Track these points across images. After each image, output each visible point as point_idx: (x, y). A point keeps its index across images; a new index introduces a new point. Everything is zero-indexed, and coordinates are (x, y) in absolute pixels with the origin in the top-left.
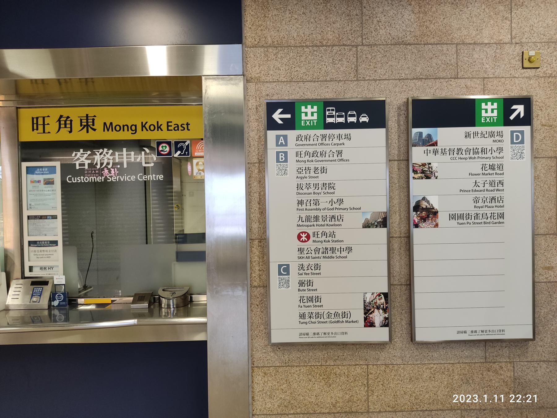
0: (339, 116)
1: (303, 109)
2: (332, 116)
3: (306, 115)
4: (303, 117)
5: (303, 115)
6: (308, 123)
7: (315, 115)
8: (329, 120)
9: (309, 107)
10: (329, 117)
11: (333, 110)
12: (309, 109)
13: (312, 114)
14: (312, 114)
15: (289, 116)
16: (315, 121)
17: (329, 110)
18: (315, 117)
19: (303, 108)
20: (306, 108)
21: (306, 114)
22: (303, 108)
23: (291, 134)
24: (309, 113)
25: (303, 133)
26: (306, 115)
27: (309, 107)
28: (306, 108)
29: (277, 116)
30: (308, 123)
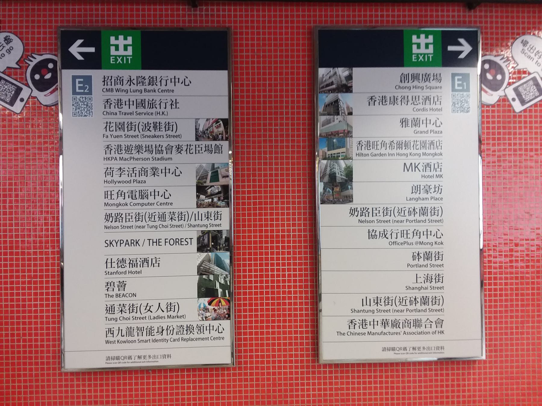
1: (113, 40)
3: (117, 48)
5: (113, 49)
6: (119, 60)
9: (121, 37)
12: (121, 41)
13: (125, 48)
14: (125, 48)
15: (92, 50)
16: (130, 58)
18: (130, 51)
19: (112, 39)
20: (117, 39)
21: (117, 48)
22: (112, 39)
23: (97, 75)
24: (122, 46)
25: (115, 73)
27: (121, 37)
28: (117, 39)
29: (75, 50)
30: (119, 60)
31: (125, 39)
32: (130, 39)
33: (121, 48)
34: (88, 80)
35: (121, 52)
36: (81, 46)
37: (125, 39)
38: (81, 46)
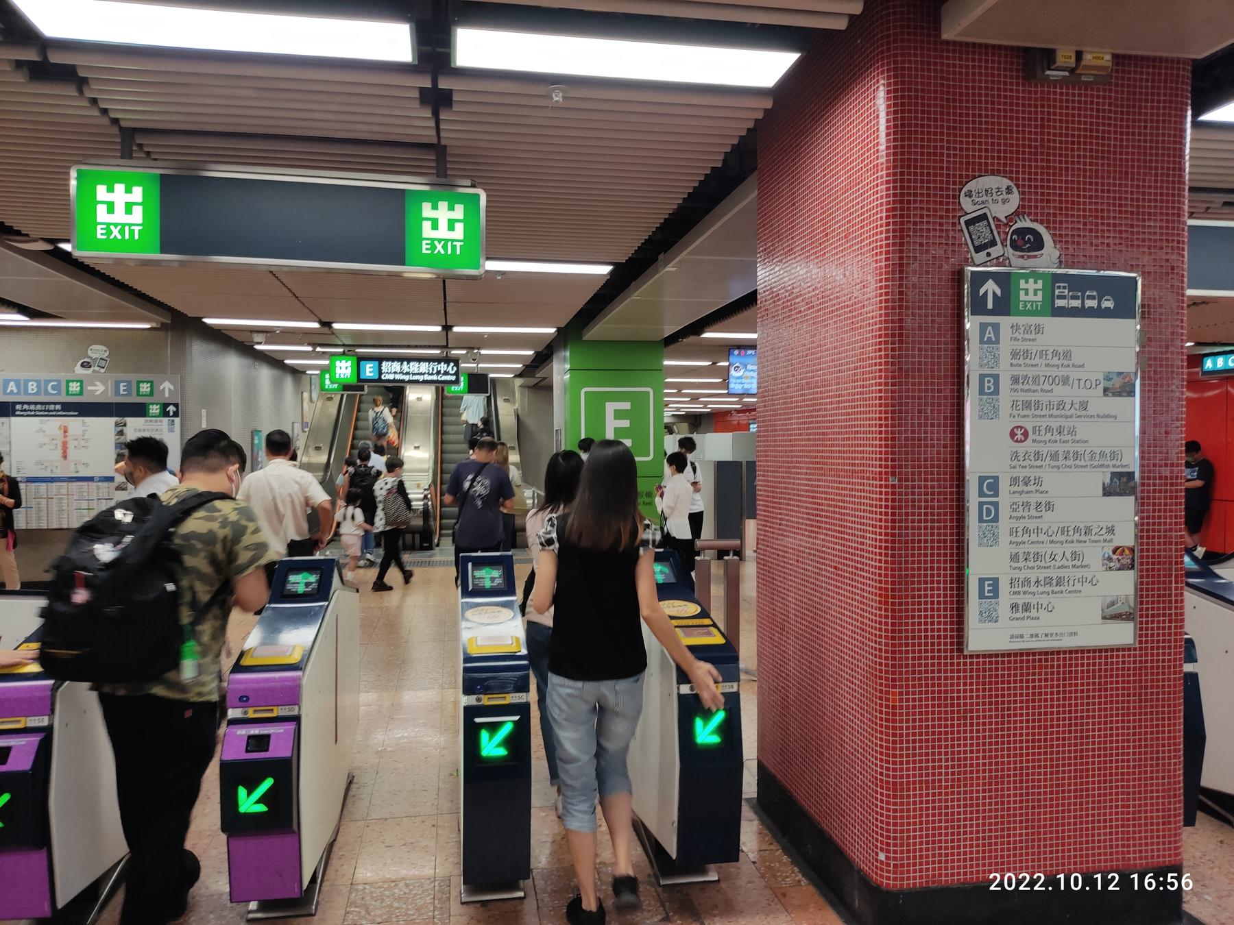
0: (1074, 298)
2: (1063, 297)
3: (1027, 294)
4: (1022, 297)
5: (1022, 293)
7: (1040, 293)
8: (1059, 303)
9: (1031, 281)
10: (1060, 297)
11: (1064, 288)
12: (1031, 285)
13: (1035, 294)
17: (1059, 287)
18: (1039, 297)
20: (1027, 282)
26: (1027, 294)
28: (1027, 282)
31: (1036, 282)
32: (1040, 282)
33: (1031, 292)
34: (996, 327)
35: (1031, 297)
36: (994, 293)
37: (1036, 282)
38: (994, 293)
